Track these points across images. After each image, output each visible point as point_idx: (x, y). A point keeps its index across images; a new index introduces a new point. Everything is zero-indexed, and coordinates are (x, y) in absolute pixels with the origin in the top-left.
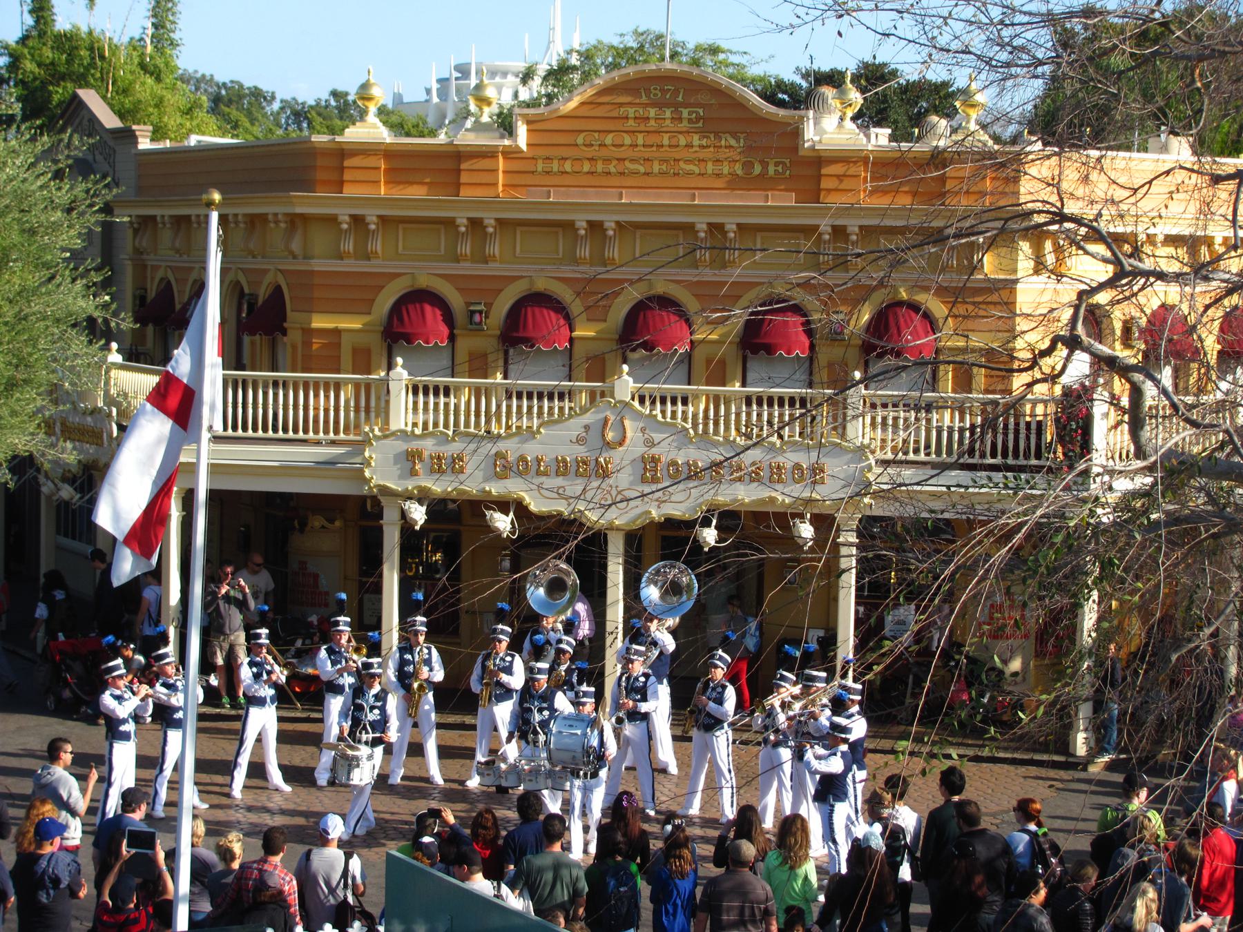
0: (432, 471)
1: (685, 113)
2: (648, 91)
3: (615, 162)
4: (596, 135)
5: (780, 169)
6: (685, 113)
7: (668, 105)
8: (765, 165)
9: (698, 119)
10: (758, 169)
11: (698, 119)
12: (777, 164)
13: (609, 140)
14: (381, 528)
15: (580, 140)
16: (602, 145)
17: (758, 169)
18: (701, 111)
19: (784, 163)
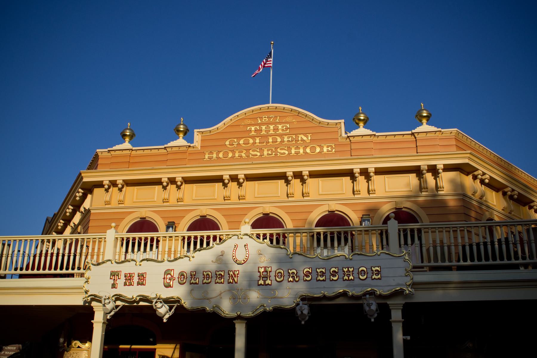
0: (125, 284)
1: (280, 127)
2: (261, 118)
3: (245, 152)
4: (236, 140)
5: (330, 149)
6: (280, 127)
7: (271, 124)
8: (321, 147)
9: (287, 129)
10: (318, 150)
11: (287, 129)
12: (328, 147)
13: (241, 142)
14: (92, 324)
15: (227, 143)
16: (239, 144)
17: (318, 150)
18: (288, 126)
19: (331, 146)
